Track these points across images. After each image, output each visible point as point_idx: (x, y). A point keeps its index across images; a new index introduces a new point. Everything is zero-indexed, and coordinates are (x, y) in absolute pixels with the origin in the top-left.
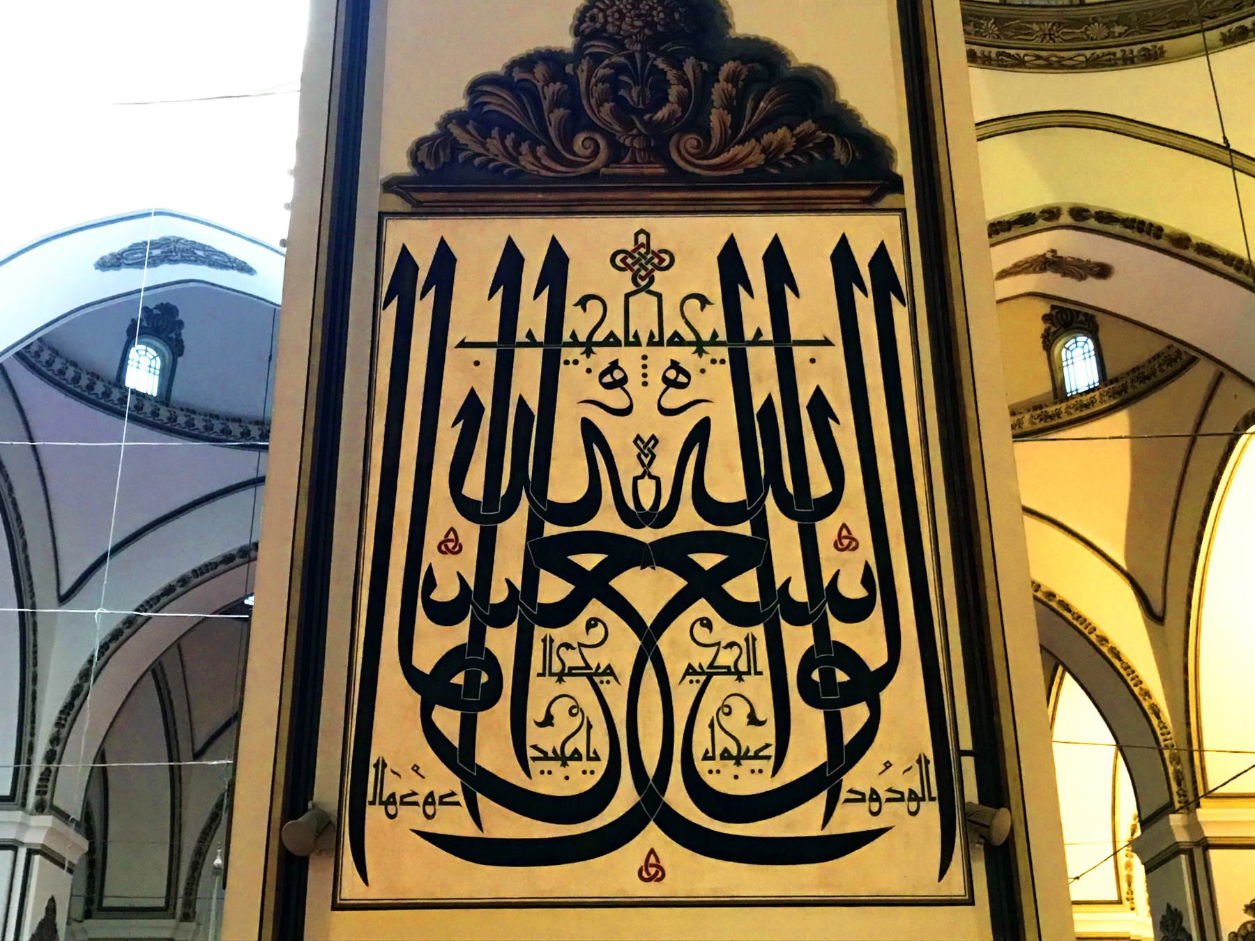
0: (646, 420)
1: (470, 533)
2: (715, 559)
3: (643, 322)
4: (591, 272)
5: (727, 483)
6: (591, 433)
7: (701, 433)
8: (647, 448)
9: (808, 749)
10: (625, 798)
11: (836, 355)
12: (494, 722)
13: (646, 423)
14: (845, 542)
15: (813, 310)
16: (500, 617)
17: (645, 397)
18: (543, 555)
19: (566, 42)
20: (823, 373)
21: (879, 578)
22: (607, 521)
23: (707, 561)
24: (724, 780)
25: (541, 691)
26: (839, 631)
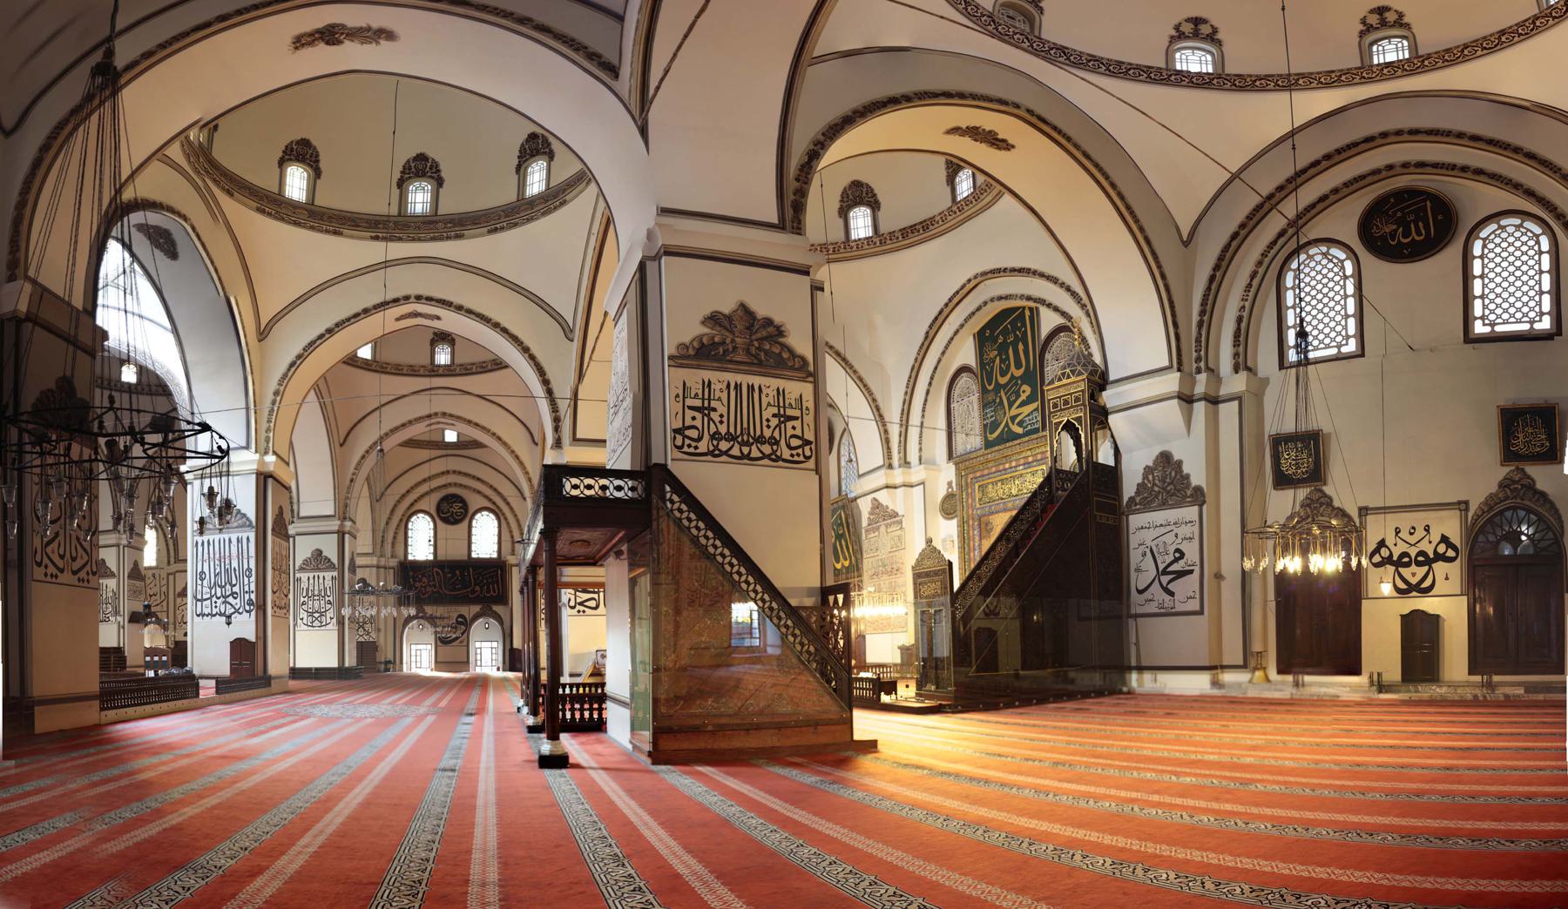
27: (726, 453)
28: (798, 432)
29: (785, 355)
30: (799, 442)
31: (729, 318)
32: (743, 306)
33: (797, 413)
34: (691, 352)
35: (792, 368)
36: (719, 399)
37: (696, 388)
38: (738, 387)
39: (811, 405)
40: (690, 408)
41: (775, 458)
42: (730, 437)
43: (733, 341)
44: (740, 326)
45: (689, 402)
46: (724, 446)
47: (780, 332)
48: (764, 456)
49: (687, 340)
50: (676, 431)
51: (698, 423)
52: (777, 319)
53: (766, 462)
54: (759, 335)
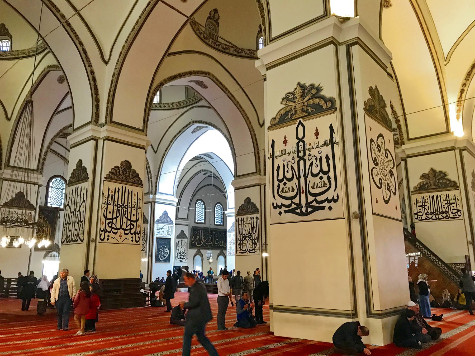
4: (245, 220)
5: (251, 233)
9: (254, 247)
17: (247, 227)
18: (243, 237)
20: (255, 225)
21: (257, 237)
27: (431, 218)
28: (455, 208)
29: (448, 182)
30: (456, 211)
31: (428, 175)
32: (432, 169)
33: (454, 201)
35: (451, 186)
36: (427, 202)
37: (420, 200)
38: (433, 197)
39: (459, 198)
40: (419, 206)
41: (447, 217)
42: (432, 213)
43: (430, 182)
44: (431, 176)
45: (418, 205)
46: (430, 216)
47: (445, 175)
48: (444, 218)
49: (416, 185)
50: (415, 214)
51: (421, 211)
52: (444, 171)
53: (445, 219)
54: (438, 178)
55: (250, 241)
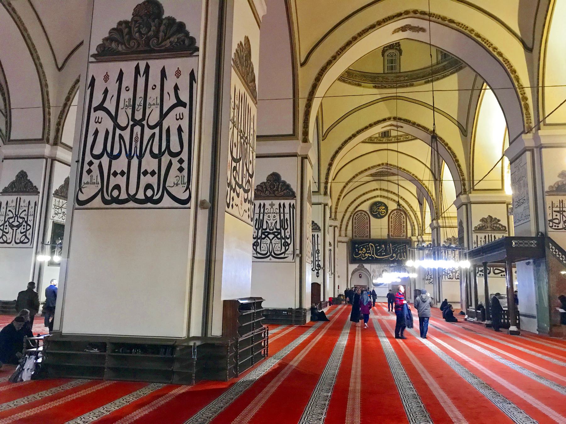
0: (272, 221)
1: (257, 231)
2: (277, 234)
3: (272, 211)
4: (267, 206)
5: (278, 227)
6: (267, 222)
7: (276, 222)
8: (272, 223)
9: (283, 250)
10: (269, 254)
11: (289, 214)
12: (258, 247)
13: (271, 221)
14: (288, 232)
15: (287, 210)
16: (259, 239)
17: (272, 218)
18: (263, 233)
19: (266, 181)
20: (287, 216)
21: (290, 236)
22: (268, 230)
23: (276, 234)
24: (276, 252)
25: (262, 245)
26: (287, 240)
34: (554, 189)
45: (554, 209)
49: (552, 184)
50: (550, 221)
51: (558, 217)
55: (275, 241)
